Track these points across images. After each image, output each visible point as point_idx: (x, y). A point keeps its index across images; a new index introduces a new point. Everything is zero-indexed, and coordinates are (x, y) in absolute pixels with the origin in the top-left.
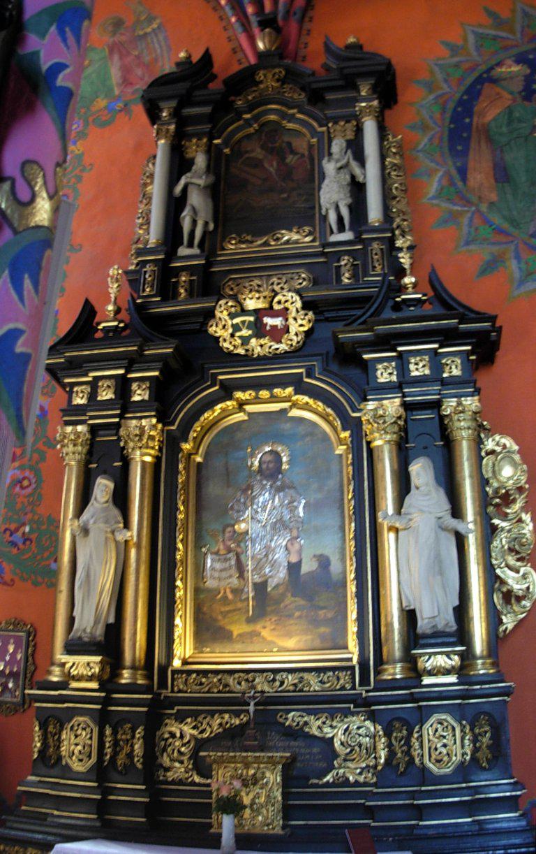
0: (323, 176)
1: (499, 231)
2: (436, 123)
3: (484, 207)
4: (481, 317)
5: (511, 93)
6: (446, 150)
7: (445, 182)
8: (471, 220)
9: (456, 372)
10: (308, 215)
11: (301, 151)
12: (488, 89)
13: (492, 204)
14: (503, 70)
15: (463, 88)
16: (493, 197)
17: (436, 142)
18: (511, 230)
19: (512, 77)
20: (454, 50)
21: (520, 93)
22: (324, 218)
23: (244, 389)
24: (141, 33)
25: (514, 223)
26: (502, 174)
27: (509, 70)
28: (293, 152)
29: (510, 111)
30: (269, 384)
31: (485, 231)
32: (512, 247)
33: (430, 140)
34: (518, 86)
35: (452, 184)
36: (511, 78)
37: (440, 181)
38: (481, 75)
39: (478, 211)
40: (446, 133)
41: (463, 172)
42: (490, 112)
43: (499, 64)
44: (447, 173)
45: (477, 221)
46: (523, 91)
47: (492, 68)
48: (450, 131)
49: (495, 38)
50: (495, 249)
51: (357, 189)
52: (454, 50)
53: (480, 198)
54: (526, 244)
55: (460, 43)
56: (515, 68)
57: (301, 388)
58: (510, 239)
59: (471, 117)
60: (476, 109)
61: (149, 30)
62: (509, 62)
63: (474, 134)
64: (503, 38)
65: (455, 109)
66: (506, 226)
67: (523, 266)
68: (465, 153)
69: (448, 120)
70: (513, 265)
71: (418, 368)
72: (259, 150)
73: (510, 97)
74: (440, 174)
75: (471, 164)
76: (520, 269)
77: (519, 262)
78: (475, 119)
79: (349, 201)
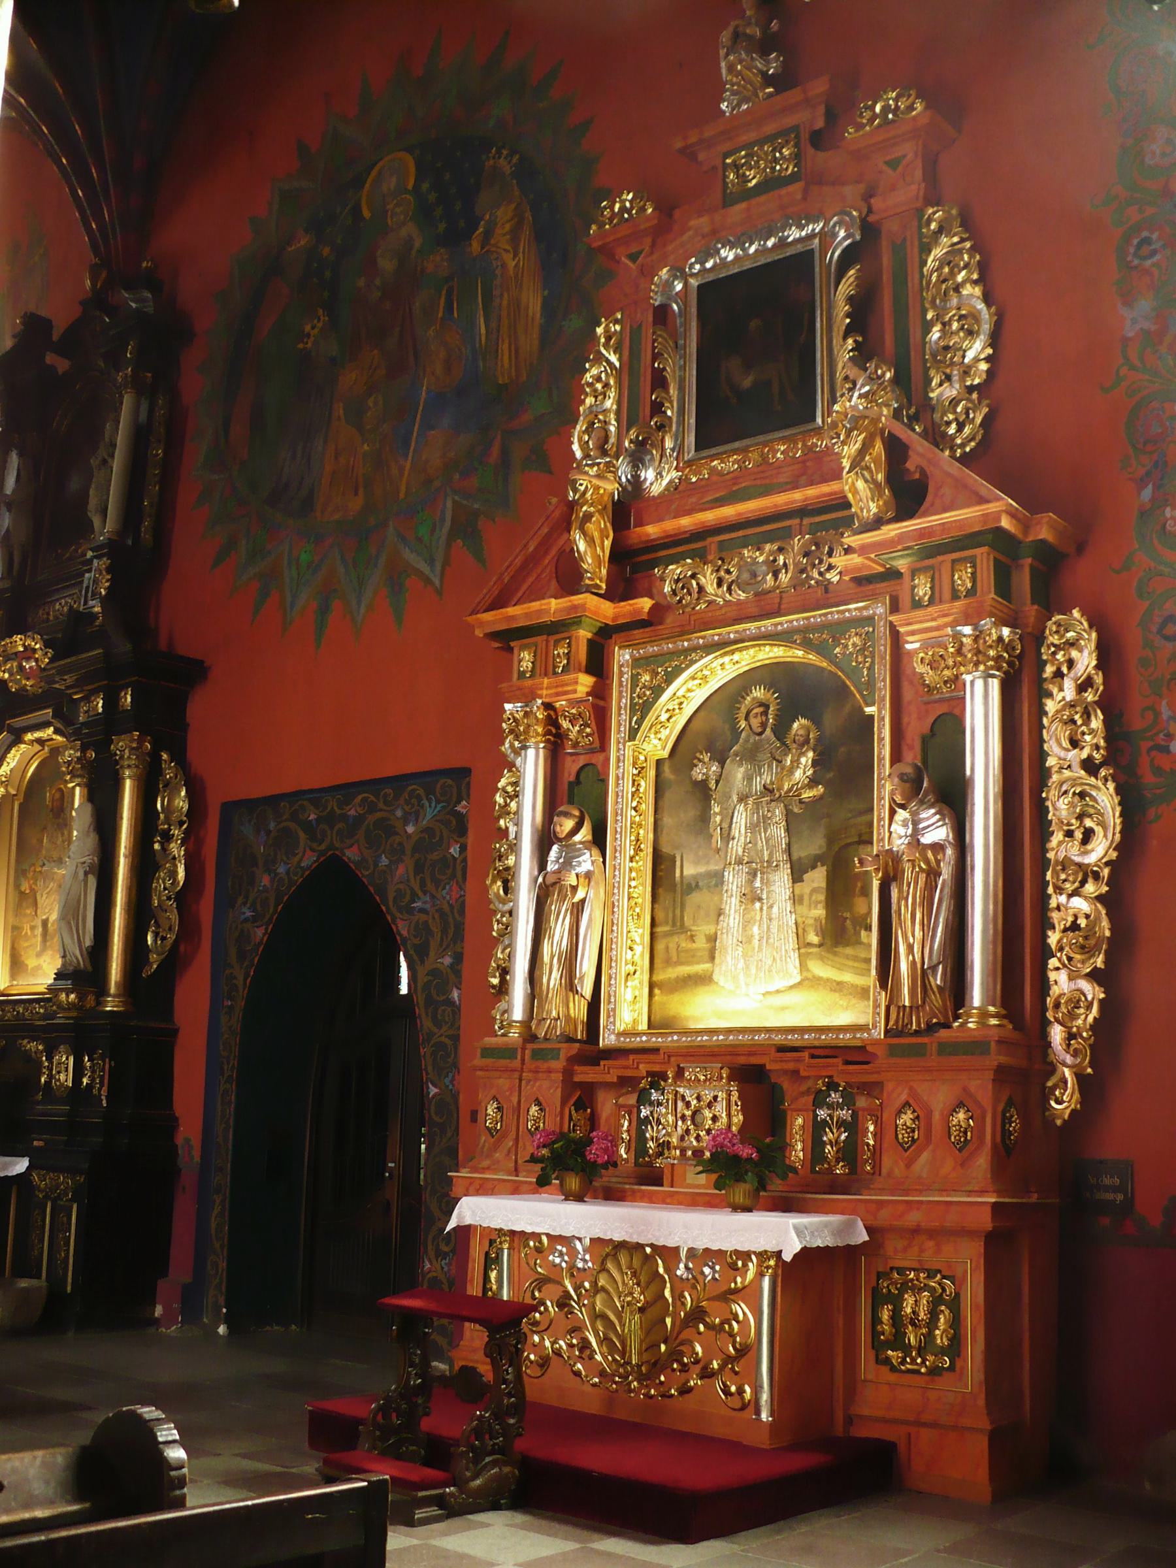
14: (293, 247)
27: (298, 245)
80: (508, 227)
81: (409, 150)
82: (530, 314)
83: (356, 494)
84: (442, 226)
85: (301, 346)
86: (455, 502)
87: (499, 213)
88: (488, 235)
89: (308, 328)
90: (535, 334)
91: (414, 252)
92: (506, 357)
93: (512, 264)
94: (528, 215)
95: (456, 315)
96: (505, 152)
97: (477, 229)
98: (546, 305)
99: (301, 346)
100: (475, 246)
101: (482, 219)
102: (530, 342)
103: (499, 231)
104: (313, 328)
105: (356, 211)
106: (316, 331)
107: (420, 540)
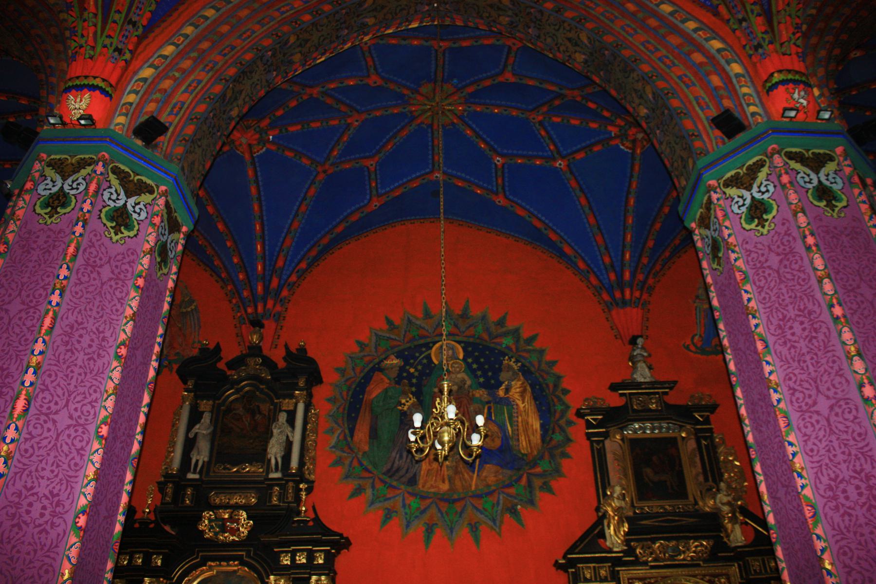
0: (272, 435)
1: (366, 470)
2: (343, 398)
3: (360, 455)
4: (336, 534)
5: (389, 379)
6: (346, 416)
7: (341, 438)
8: (351, 462)
9: (321, 561)
10: (261, 457)
11: (264, 412)
12: (378, 376)
13: (365, 453)
14: (388, 362)
15: (362, 375)
16: (366, 448)
17: (341, 410)
18: (373, 469)
19: (392, 367)
20: (363, 346)
21: (394, 379)
22: (269, 460)
23: (213, 561)
24: (184, 310)
25: (375, 466)
26: (374, 434)
28: (260, 413)
29: (386, 391)
30: (228, 559)
31: (358, 470)
32: (371, 481)
33: (338, 409)
34: (394, 374)
35: (345, 438)
36: (392, 368)
37: (338, 437)
38: (374, 366)
39: (356, 456)
40: (347, 405)
41: (352, 431)
42: (375, 391)
43: (386, 358)
44: (343, 431)
45: (355, 462)
46: (397, 377)
47: (382, 361)
48: (350, 403)
49: (389, 339)
50: (361, 482)
51: (289, 444)
52: (363, 346)
53: (359, 448)
54: (379, 479)
55: (366, 343)
56: (395, 361)
57: (243, 563)
58: (372, 475)
59: (363, 395)
60: (367, 389)
61: (189, 309)
62: (393, 357)
63: (363, 406)
64: (392, 339)
65: (355, 388)
66: (370, 467)
67: (375, 492)
68: (356, 418)
69: (350, 396)
70: (369, 492)
71: (302, 559)
72: (241, 409)
73: (388, 381)
74: (339, 432)
75: (357, 427)
76: (373, 494)
77: (373, 490)
78: (366, 396)
79: (283, 453)
80: (518, 390)
81: (459, 342)
82: (534, 427)
83: (444, 482)
84: (482, 380)
85: (400, 408)
86: (503, 497)
87: (513, 383)
88: (507, 390)
89: (403, 401)
90: (539, 437)
91: (466, 386)
92: (524, 443)
93: (521, 406)
94: (529, 388)
95: (493, 418)
96: (513, 360)
97: (501, 386)
98: (542, 426)
99: (400, 408)
100: (501, 393)
101: (503, 382)
102: (536, 439)
103: (513, 390)
104: (407, 402)
105: (429, 357)
106: (409, 404)
107: (486, 510)
